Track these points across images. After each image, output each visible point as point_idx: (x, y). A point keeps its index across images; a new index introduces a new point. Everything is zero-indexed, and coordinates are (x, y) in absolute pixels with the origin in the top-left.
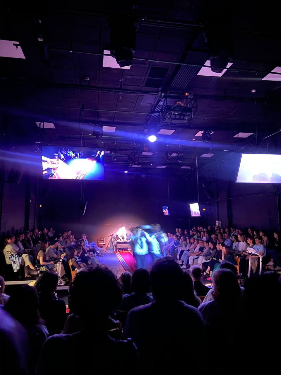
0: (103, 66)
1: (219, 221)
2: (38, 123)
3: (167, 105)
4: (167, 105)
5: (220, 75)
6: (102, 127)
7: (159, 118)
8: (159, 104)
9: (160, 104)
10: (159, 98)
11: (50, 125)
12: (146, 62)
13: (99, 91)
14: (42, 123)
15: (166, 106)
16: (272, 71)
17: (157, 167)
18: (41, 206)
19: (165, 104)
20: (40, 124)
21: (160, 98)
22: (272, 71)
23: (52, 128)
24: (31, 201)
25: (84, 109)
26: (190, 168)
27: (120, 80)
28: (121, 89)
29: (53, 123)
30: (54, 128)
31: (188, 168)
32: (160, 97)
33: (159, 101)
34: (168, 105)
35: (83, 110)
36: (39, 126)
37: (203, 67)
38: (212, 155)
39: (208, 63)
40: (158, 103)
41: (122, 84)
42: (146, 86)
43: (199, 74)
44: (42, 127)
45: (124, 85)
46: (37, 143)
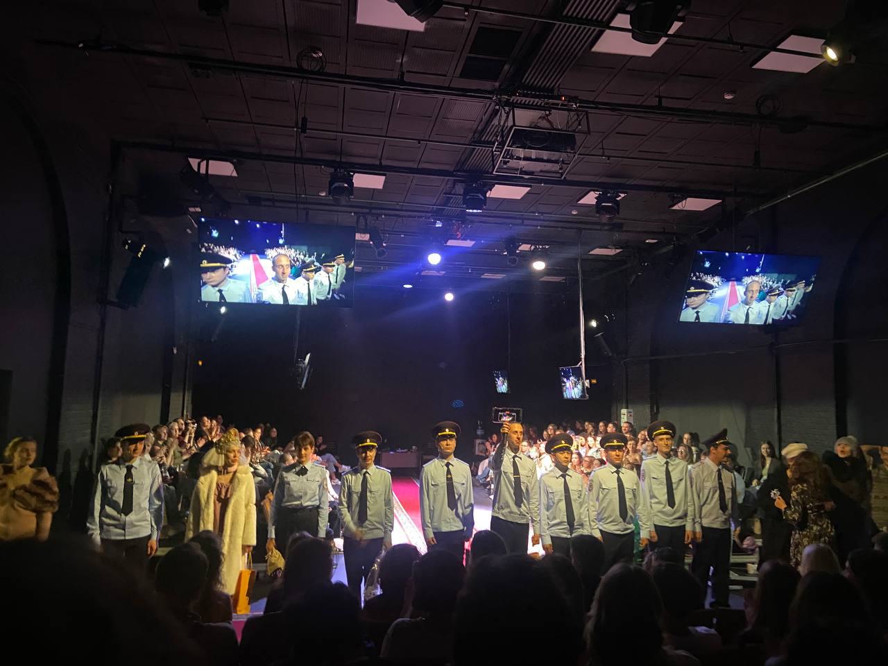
0: (358, 22)
1: (630, 410)
2: (194, 162)
3: (514, 125)
4: (514, 125)
5: (646, 50)
6: (353, 176)
7: (493, 156)
8: (493, 123)
9: (495, 122)
10: (495, 106)
11: (223, 169)
12: (466, 13)
13: (349, 87)
14: (205, 162)
15: (511, 127)
16: (779, 47)
17: (483, 277)
18: (200, 363)
19: (510, 123)
20: (199, 164)
21: (497, 107)
22: (779, 47)
23: (230, 175)
24: (175, 351)
25: (308, 131)
26: (563, 280)
27: (398, 59)
28: (401, 81)
29: (231, 162)
30: (235, 174)
31: (558, 280)
32: (497, 104)
33: (495, 112)
34: (516, 124)
35: (304, 131)
36: (196, 170)
37: (608, 32)
38: (618, 251)
39: (623, 20)
40: (491, 122)
41: (404, 70)
42: (461, 76)
43: (593, 49)
44: (203, 171)
45: (408, 72)
46: (192, 209)
